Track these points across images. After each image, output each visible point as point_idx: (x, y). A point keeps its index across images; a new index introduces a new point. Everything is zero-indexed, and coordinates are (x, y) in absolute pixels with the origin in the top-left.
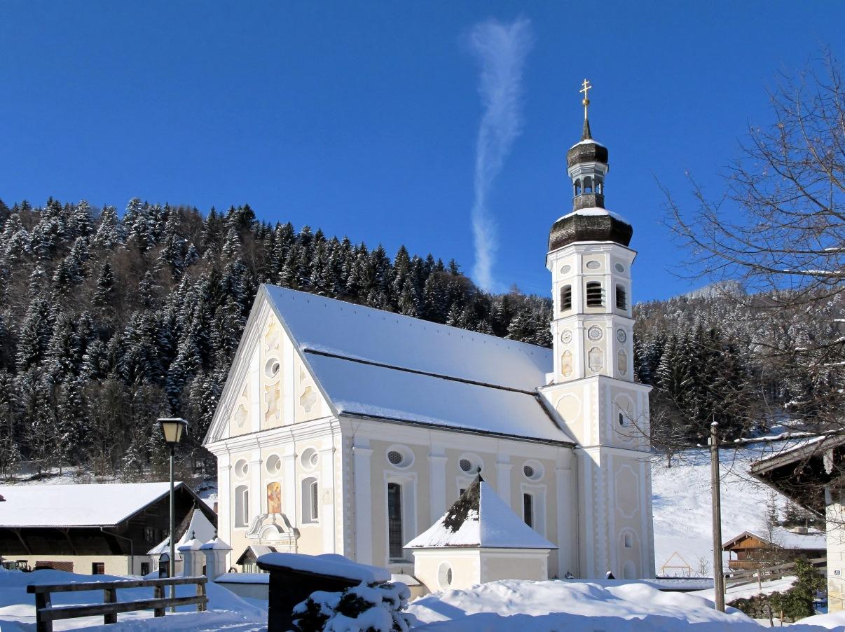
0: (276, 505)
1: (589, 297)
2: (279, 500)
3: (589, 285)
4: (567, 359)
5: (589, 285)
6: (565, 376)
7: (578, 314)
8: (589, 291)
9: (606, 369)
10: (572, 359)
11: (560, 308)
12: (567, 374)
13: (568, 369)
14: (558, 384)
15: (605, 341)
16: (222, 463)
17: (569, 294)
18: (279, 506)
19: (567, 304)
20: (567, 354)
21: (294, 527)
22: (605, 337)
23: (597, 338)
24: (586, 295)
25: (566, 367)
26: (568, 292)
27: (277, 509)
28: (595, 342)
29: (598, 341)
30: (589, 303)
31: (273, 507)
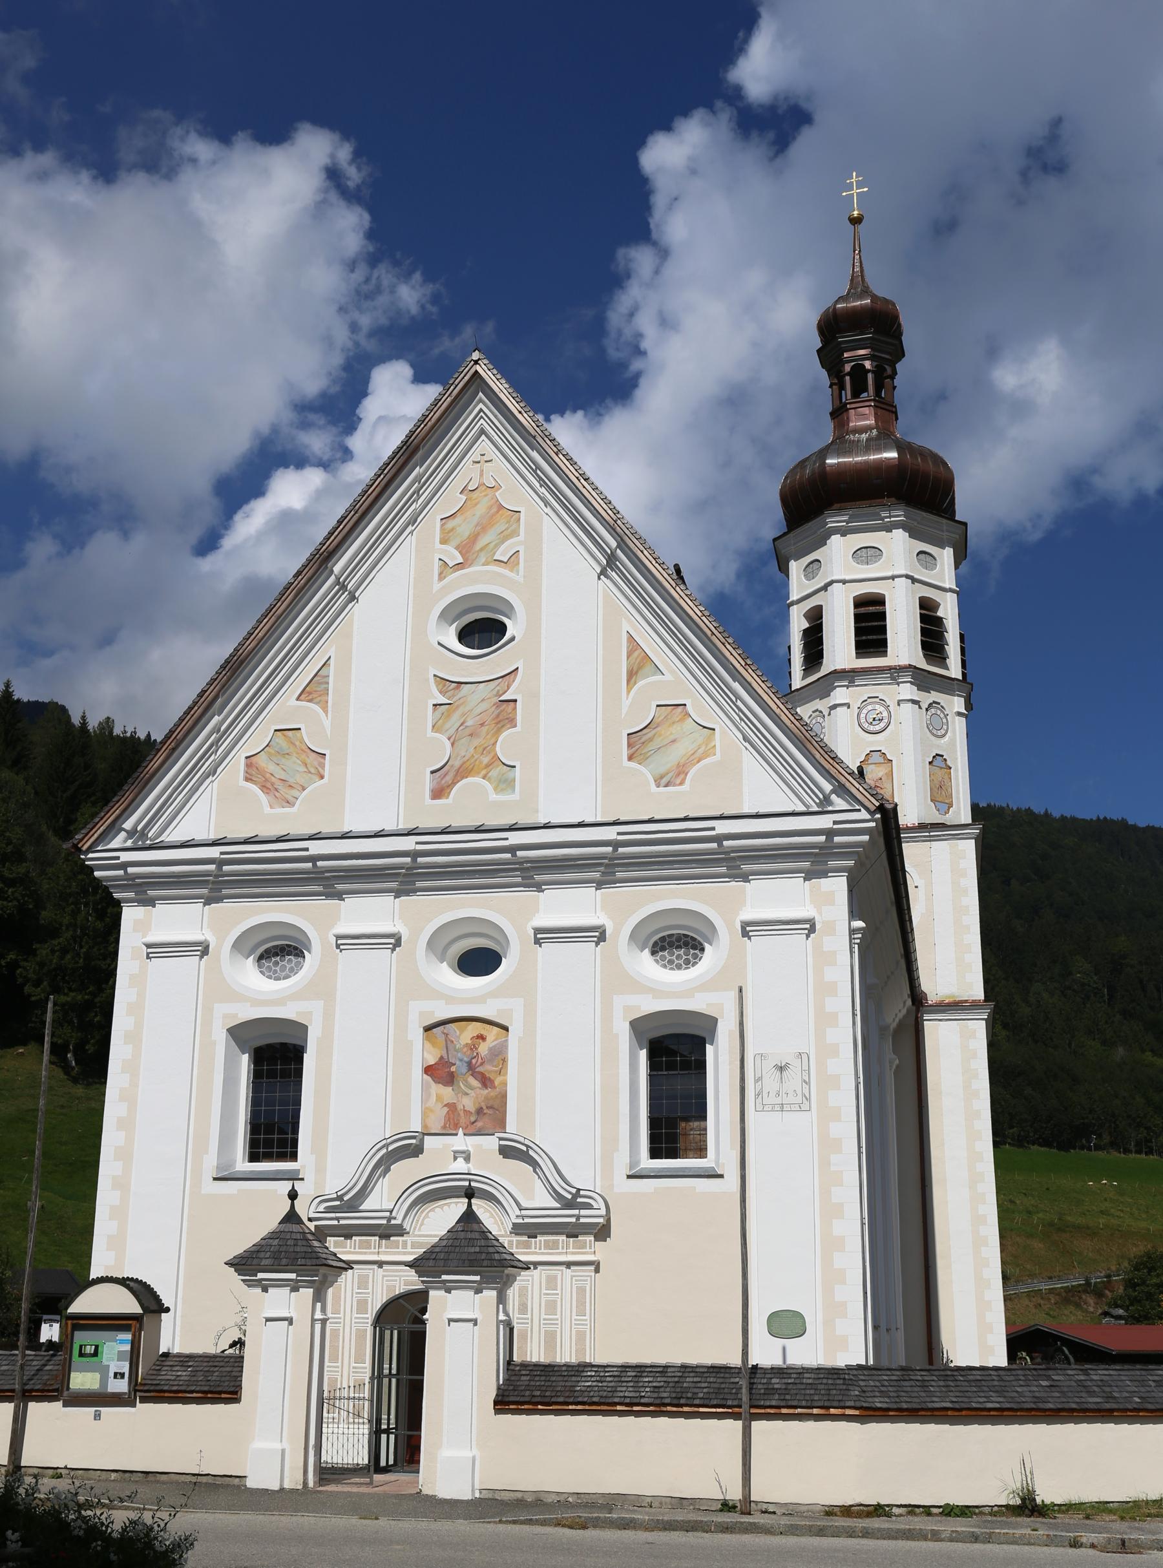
0: (468, 1104)
9: (959, 813)
10: (890, 774)
15: (953, 740)
16: (137, 926)
20: (876, 757)
22: (954, 732)
31: (452, 1107)
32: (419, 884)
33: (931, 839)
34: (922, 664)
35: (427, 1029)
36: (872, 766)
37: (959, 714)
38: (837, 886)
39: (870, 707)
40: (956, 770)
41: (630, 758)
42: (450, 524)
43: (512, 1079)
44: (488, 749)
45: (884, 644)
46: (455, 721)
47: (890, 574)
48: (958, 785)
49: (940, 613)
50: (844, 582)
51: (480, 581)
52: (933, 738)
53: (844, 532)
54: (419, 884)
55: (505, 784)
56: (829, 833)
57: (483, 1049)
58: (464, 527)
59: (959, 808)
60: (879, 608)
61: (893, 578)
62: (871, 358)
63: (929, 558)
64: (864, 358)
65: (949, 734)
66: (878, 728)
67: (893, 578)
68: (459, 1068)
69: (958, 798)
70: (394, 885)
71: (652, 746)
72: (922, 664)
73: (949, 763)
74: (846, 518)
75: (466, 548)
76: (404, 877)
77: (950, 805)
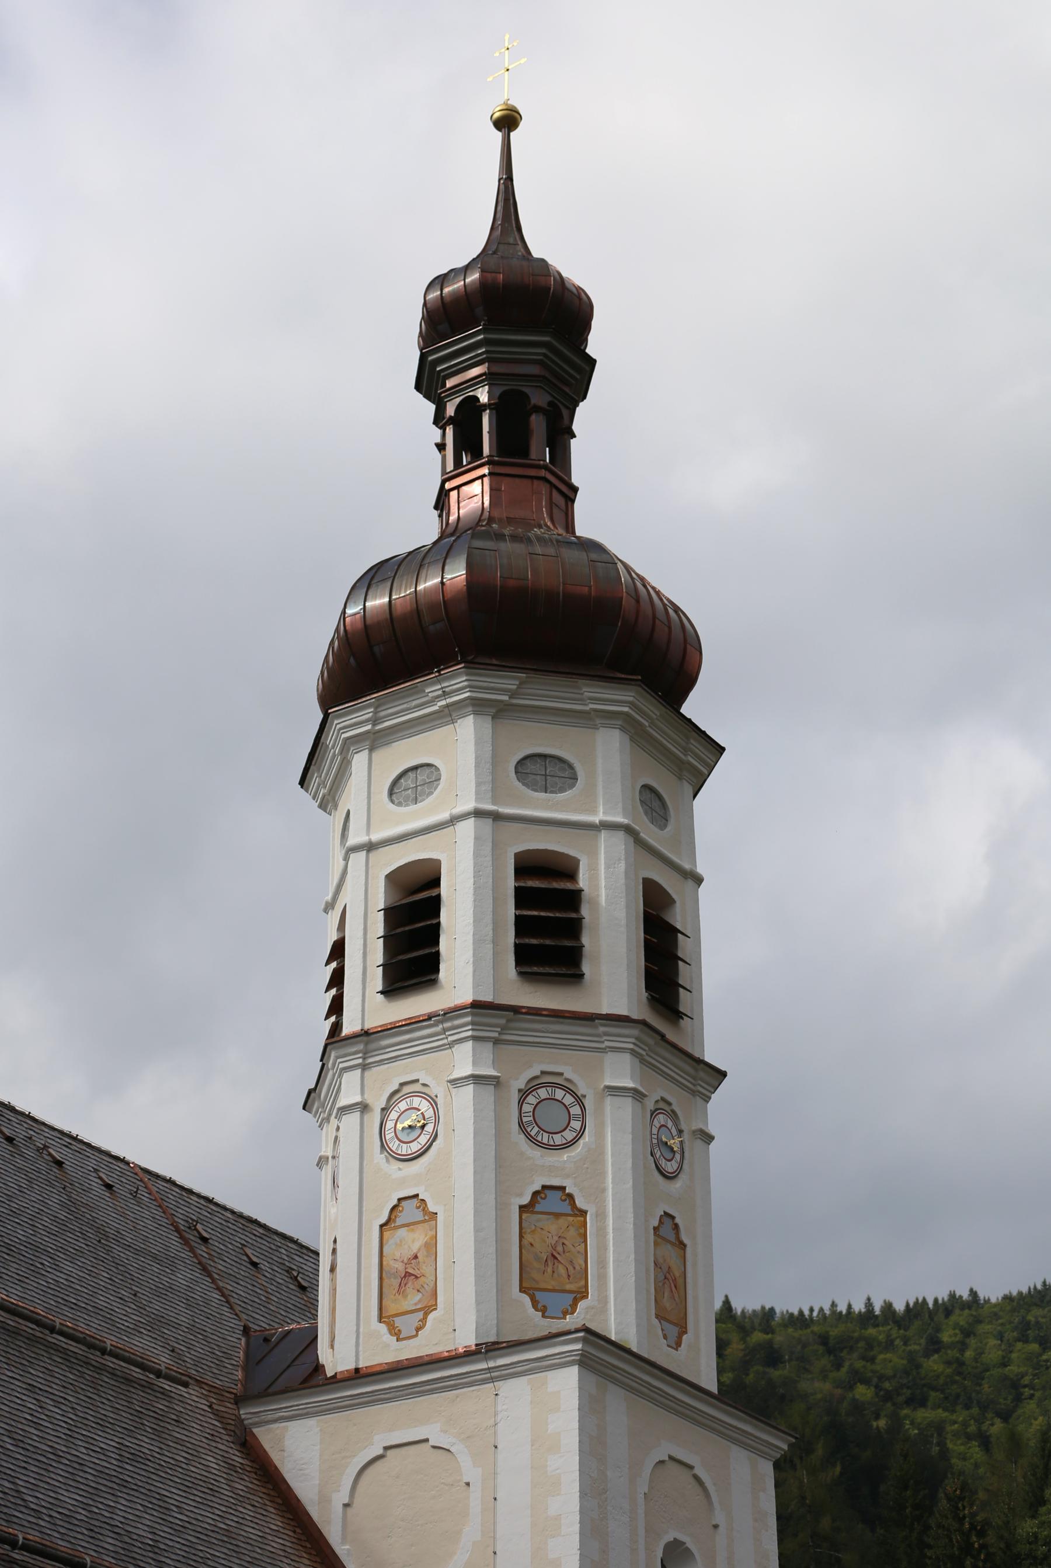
1: (522, 925)
3: (529, 866)
4: (408, 1241)
5: (529, 866)
6: (395, 1332)
7: (476, 1005)
8: (522, 897)
10: (431, 1246)
11: (377, 980)
12: (407, 1325)
13: (413, 1299)
14: (358, 1375)
15: (596, 1155)
17: (434, 905)
22: (600, 1135)
23: (558, 1139)
25: (404, 1284)
29: (565, 1156)
33: (494, 1377)
36: (402, 1232)
37: (614, 1091)
39: (403, 1106)
40: (601, 1215)
47: (445, 816)
48: (602, 1248)
50: (370, 847)
52: (536, 1153)
59: (604, 1301)
60: (433, 893)
61: (454, 820)
62: (489, 378)
63: (422, 776)
64: (475, 382)
65: (587, 1137)
66: (415, 1147)
69: (602, 1277)
73: (580, 1203)
74: (368, 714)
77: (582, 1294)
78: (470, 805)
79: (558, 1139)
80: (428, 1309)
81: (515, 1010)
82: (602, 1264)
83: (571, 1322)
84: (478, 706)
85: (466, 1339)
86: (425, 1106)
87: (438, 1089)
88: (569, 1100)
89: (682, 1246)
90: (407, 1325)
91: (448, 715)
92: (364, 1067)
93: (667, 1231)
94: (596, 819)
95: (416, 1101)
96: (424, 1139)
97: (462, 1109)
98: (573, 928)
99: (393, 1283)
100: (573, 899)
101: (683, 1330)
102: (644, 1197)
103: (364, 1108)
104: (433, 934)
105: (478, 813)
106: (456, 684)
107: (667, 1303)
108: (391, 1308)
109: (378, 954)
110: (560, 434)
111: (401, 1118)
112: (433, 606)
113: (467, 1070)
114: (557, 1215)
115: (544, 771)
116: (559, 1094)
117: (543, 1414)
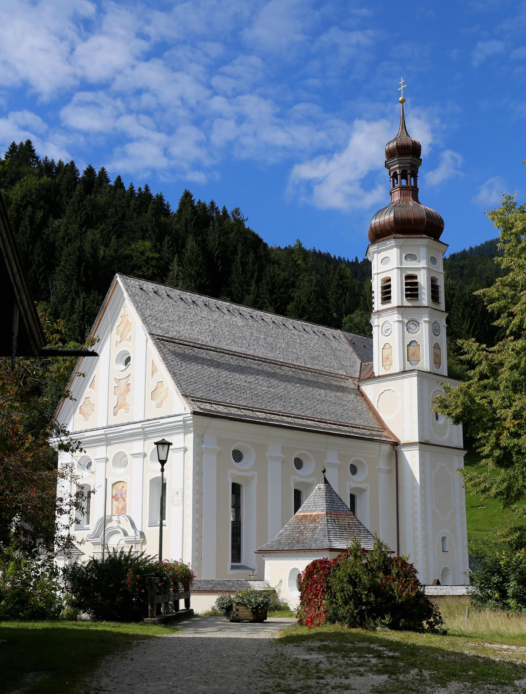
0: (120, 507)
1: (407, 290)
2: (124, 500)
3: (408, 277)
4: (387, 352)
5: (408, 277)
7: (398, 307)
9: (423, 364)
10: (391, 353)
12: (387, 367)
13: (388, 363)
15: (421, 335)
17: (389, 286)
18: (124, 508)
19: (386, 297)
21: (140, 530)
22: (422, 330)
23: (414, 331)
24: (404, 287)
25: (386, 359)
26: (388, 284)
27: (122, 511)
28: (413, 335)
29: (415, 334)
30: (407, 296)
31: (117, 507)
32: (112, 442)
34: (406, 303)
35: (113, 485)
38: (191, 436)
40: (423, 345)
41: (152, 400)
42: (119, 328)
43: (127, 499)
44: (124, 399)
45: (390, 298)
46: (118, 392)
47: (391, 268)
49: (418, 280)
50: (378, 274)
51: (122, 347)
53: (379, 252)
54: (112, 442)
55: (127, 410)
56: (184, 421)
57: (123, 491)
58: (121, 329)
61: (393, 269)
66: (388, 334)
67: (393, 269)
68: (119, 496)
69: (423, 357)
70: (104, 443)
71: (157, 395)
72: (406, 303)
74: (376, 247)
75: (121, 336)
76: (107, 441)
77: (419, 361)
78: (396, 266)
79: (414, 331)
80: (391, 365)
81: (406, 307)
82: (423, 355)
83: (416, 367)
84: (397, 246)
85: (398, 371)
86: (389, 326)
87: (391, 323)
88: (416, 323)
89: (440, 349)
90: (387, 367)
91: (391, 248)
92: (378, 318)
93: (437, 346)
94: (421, 266)
95: (388, 325)
96: (389, 332)
97: (396, 328)
98: (417, 290)
99: (384, 359)
100: (416, 284)
101: (440, 365)
102: (431, 340)
103: (379, 326)
104: (389, 292)
105: (397, 268)
106: (392, 242)
107: (437, 360)
108: (384, 364)
109: (380, 295)
110: (415, 175)
111: (385, 327)
112: (387, 223)
113: (397, 320)
114: (414, 346)
115: (411, 257)
116: (414, 322)
117: (411, 383)
